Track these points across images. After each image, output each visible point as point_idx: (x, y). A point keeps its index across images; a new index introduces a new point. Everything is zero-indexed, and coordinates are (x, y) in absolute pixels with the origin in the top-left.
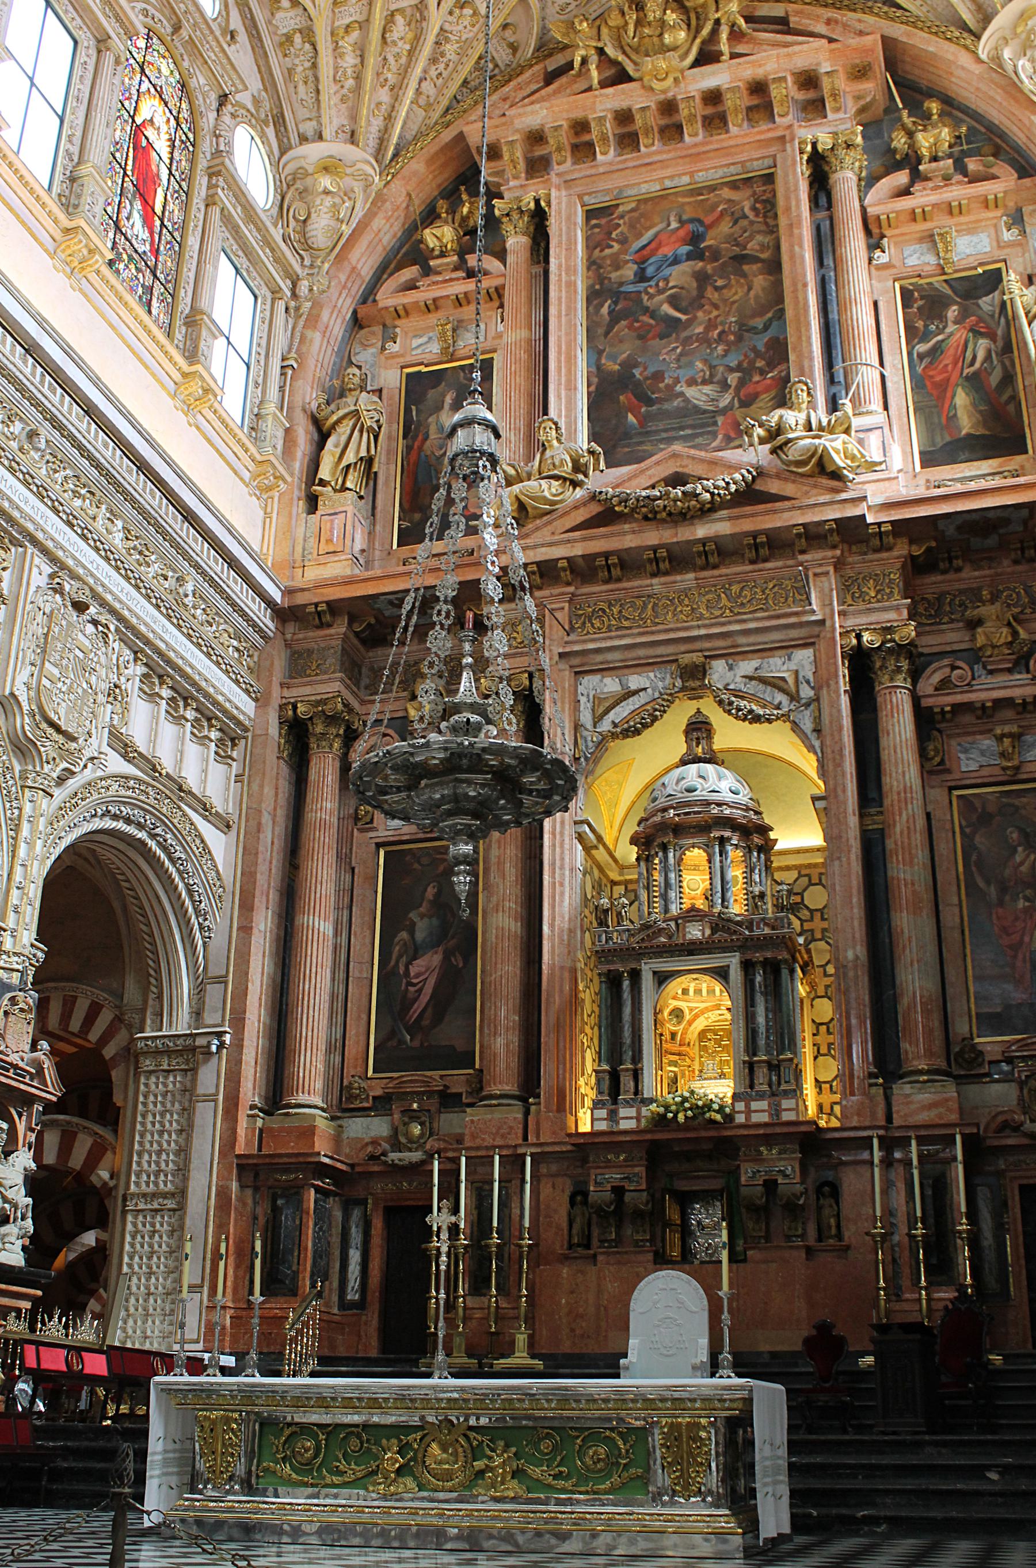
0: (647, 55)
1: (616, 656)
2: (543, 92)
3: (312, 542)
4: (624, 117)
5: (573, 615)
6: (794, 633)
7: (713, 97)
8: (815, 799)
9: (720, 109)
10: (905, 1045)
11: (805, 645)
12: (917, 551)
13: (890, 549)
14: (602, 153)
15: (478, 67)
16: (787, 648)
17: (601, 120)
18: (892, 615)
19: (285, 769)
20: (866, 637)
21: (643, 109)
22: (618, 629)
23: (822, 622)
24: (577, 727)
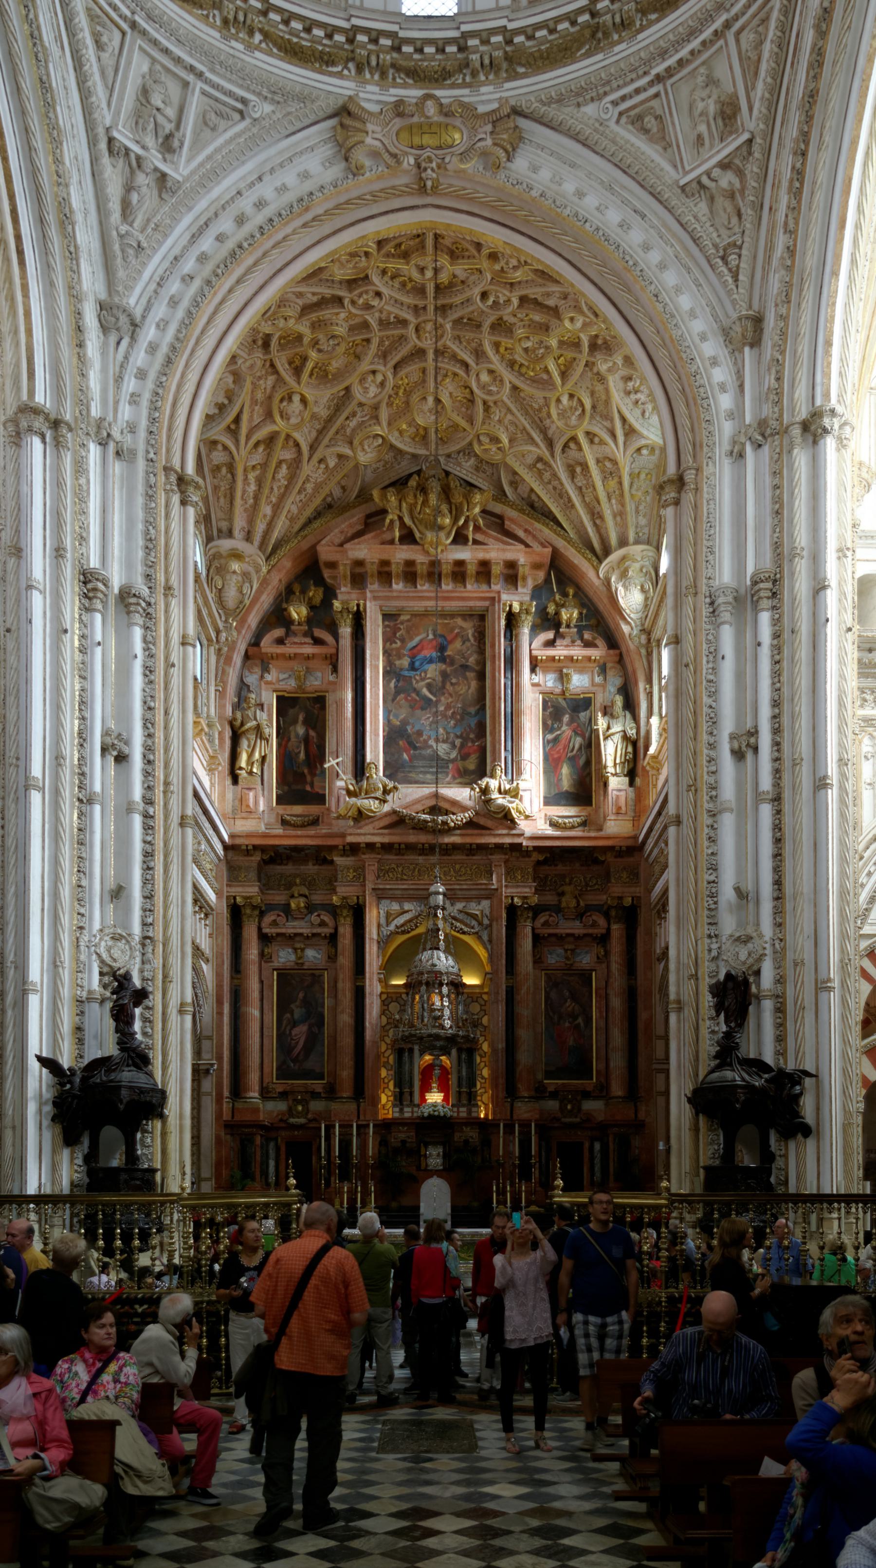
0: (426, 527)
1: (399, 892)
2: (366, 537)
3: (237, 803)
4: (410, 563)
5: (380, 870)
6: (483, 892)
7: (460, 563)
8: (486, 974)
9: (462, 569)
10: (519, 1086)
11: (487, 898)
12: (541, 858)
13: (530, 856)
14: (397, 584)
15: (325, 499)
16: (479, 899)
17: (398, 563)
18: (527, 890)
19: (226, 930)
20: (516, 900)
21: (422, 563)
22: (402, 879)
23: (496, 890)
24: (379, 926)
